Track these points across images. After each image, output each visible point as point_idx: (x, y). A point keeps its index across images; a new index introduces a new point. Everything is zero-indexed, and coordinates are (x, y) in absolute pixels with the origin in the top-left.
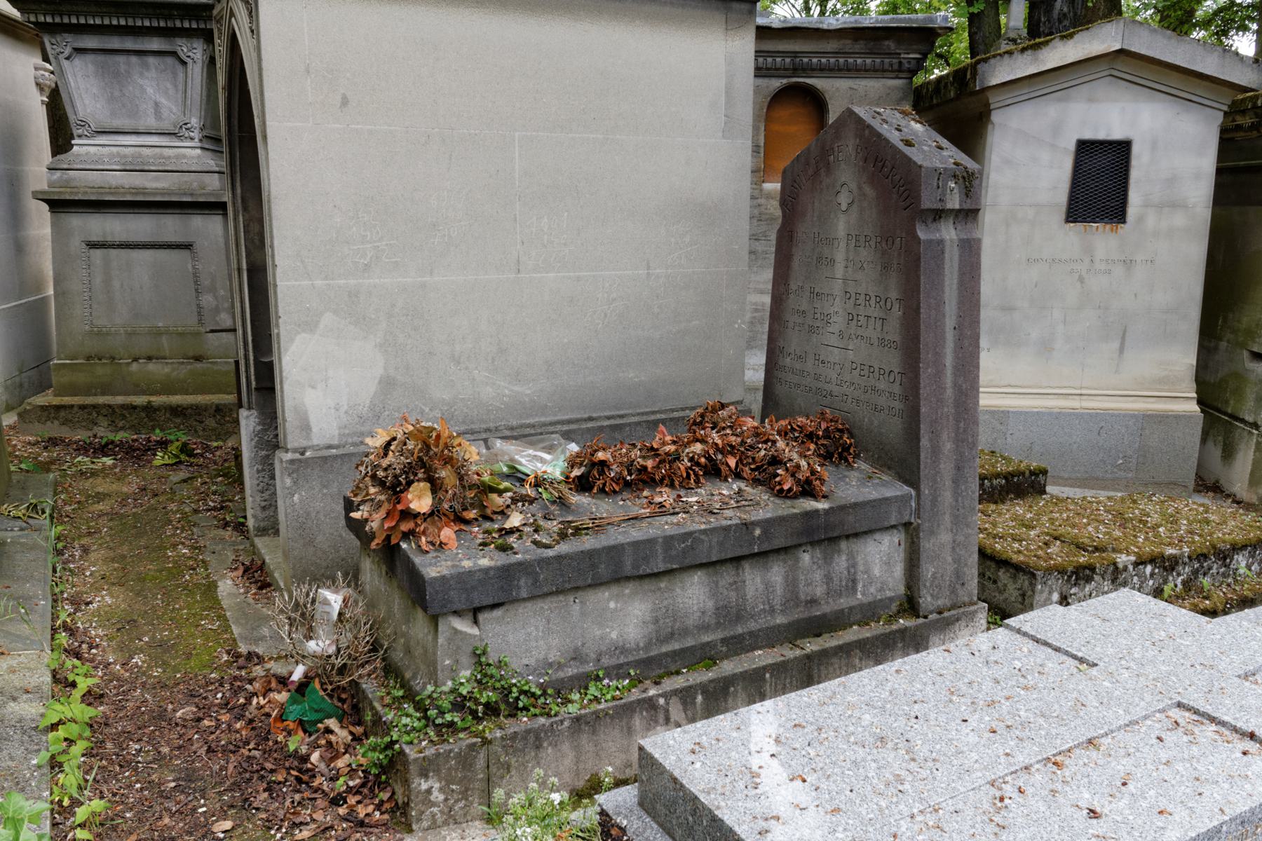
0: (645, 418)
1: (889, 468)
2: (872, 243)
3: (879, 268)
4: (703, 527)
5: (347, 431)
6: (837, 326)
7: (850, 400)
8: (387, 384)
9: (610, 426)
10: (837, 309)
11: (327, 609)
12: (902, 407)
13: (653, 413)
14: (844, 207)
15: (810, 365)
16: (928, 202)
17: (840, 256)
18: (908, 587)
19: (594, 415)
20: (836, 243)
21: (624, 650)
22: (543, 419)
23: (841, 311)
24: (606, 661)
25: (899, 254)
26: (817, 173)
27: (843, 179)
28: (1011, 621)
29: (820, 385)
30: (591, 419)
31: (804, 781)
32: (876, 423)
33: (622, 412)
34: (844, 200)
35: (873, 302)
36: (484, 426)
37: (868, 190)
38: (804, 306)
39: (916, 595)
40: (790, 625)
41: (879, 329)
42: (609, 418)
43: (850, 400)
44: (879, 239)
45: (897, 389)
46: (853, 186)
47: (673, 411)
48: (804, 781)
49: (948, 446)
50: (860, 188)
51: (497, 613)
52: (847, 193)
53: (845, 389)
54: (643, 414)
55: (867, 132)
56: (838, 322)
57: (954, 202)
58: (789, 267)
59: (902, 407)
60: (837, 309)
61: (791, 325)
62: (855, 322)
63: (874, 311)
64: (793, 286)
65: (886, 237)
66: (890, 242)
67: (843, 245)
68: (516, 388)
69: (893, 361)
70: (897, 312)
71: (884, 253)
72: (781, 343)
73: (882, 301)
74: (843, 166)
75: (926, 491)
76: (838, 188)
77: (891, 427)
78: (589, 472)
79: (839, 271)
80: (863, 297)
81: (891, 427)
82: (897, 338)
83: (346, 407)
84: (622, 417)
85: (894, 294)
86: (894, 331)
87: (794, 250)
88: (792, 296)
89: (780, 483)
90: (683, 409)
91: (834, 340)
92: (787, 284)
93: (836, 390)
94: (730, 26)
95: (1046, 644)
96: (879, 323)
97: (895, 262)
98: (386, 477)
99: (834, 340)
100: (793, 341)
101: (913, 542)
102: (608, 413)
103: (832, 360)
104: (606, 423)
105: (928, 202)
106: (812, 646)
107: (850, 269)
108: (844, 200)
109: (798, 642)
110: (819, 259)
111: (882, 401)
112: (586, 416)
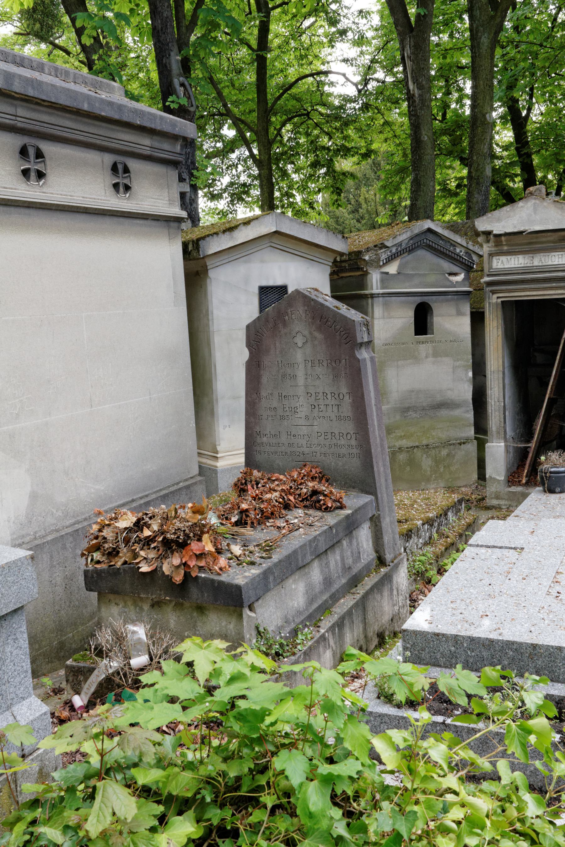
0: (159, 494)
1: (354, 488)
2: (325, 364)
3: (331, 377)
4: (318, 533)
5: (15, 536)
6: (303, 413)
7: (318, 454)
8: (34, 497)
9: (145, 503)
10: (303, 406)
11: (136, 637)
12: (358, 451)
13: (161, 490)
14: (300, 344)
15: (284, 439)
16: (359, 341)
17: (300, 373)
18: (377, 552)
19: (135, 498)
20: (296, 366)
21: (299, 613)
22: (111, 506)
23: (305, 404)
24: (298, 620)
25: (346, 368)
26: (275, 325)
27: (297, 329)
28: (471, 542)
29: (294, 449)
30: (133, 501)
31: (487, 616)
32: (340, 464)
33: (147, 493)
34: (299, 341)
35: (329, 396)
36: (83, 517)
37: (317, 334)
38: (275, 404)
39: (382, 554)
40: (349, 580)
41: (336, 411)
42: (141, 498)
43: (318, 454)
44: (329, 361)
45: (353, 442)
46: (306, 333)
47: (169, 487)
48: (487, 616)
49: (382, 469)
50: (311, 333)
51: (260, 601)
52: (301, 337)
53: (314, 449)
54: (157, 491)
55: (312, 303)
56: (303, 411)
57: (366, 340)
58: (259, 382)
59: (358, 451)
60: (303, 406)
61: (265, 417)
62: (317, 409)
63: (331, 401)
64: (263, 393)
65: (334, 360)
66: (338, 362)
67: (302, 367)
68: (97, 487)
69: (349, 427)
70: (348, 400)
71: (334, 369)
72: (258, 429)
73: (337, 396)
74: (296, 322)
75: (379, 496)
76: (294, 334)
77: (353, 464)
78: (242, 518)
79: (301, 380)
80: (321, 394)
81: (353, 464)
82: (350, 414)
83: (13, 519)
84: (147, 496)
85: (344, 390)
86: (347, 409)
87: (262, 372)
88: (263, 400)
89: (324, 504)
90: (173, 485)
91: (302, 422)
92: (258, 392)
93: (306, 450)
94: (171, 238)
95: (494, 547)
96: (335, 409)
97: (343, 372)
98: (178, 537)
99: (302, 422)
100: (268, 426)
101: (376, 525)
102: (140, 495)
103: (302, 433)
104: (142, 501)
105: (359, 341)
106: (361, 591)
107: (309, 380)
108: (299, 341)
109: (352, 591)
110: (284, 376)
111: (343, 451)
112: (131, 499)
